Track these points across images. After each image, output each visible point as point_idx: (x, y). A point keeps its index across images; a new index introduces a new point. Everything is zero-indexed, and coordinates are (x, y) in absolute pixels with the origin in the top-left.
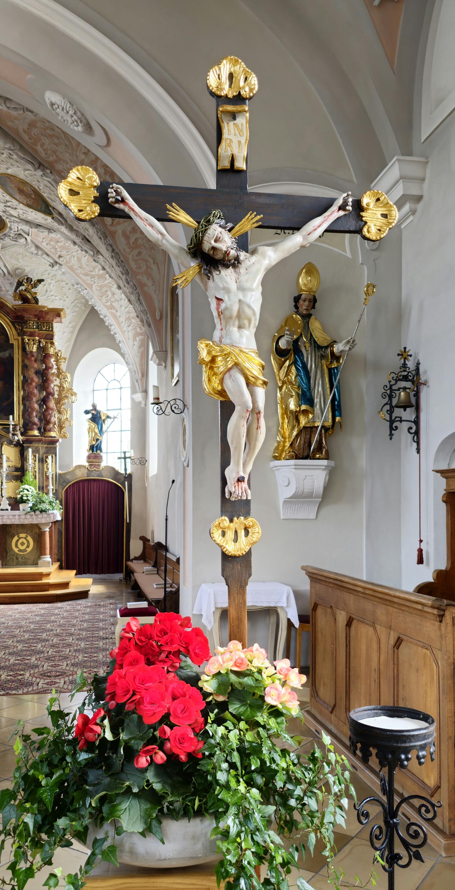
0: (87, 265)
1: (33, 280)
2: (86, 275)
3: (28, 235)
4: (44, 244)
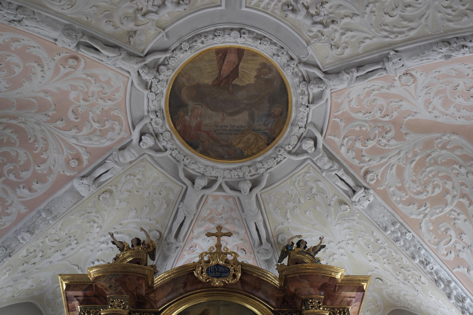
0: (414, 181)
1: (309, 246)
2: (410, 202)
3: (322, 133)
4: (343, 150)
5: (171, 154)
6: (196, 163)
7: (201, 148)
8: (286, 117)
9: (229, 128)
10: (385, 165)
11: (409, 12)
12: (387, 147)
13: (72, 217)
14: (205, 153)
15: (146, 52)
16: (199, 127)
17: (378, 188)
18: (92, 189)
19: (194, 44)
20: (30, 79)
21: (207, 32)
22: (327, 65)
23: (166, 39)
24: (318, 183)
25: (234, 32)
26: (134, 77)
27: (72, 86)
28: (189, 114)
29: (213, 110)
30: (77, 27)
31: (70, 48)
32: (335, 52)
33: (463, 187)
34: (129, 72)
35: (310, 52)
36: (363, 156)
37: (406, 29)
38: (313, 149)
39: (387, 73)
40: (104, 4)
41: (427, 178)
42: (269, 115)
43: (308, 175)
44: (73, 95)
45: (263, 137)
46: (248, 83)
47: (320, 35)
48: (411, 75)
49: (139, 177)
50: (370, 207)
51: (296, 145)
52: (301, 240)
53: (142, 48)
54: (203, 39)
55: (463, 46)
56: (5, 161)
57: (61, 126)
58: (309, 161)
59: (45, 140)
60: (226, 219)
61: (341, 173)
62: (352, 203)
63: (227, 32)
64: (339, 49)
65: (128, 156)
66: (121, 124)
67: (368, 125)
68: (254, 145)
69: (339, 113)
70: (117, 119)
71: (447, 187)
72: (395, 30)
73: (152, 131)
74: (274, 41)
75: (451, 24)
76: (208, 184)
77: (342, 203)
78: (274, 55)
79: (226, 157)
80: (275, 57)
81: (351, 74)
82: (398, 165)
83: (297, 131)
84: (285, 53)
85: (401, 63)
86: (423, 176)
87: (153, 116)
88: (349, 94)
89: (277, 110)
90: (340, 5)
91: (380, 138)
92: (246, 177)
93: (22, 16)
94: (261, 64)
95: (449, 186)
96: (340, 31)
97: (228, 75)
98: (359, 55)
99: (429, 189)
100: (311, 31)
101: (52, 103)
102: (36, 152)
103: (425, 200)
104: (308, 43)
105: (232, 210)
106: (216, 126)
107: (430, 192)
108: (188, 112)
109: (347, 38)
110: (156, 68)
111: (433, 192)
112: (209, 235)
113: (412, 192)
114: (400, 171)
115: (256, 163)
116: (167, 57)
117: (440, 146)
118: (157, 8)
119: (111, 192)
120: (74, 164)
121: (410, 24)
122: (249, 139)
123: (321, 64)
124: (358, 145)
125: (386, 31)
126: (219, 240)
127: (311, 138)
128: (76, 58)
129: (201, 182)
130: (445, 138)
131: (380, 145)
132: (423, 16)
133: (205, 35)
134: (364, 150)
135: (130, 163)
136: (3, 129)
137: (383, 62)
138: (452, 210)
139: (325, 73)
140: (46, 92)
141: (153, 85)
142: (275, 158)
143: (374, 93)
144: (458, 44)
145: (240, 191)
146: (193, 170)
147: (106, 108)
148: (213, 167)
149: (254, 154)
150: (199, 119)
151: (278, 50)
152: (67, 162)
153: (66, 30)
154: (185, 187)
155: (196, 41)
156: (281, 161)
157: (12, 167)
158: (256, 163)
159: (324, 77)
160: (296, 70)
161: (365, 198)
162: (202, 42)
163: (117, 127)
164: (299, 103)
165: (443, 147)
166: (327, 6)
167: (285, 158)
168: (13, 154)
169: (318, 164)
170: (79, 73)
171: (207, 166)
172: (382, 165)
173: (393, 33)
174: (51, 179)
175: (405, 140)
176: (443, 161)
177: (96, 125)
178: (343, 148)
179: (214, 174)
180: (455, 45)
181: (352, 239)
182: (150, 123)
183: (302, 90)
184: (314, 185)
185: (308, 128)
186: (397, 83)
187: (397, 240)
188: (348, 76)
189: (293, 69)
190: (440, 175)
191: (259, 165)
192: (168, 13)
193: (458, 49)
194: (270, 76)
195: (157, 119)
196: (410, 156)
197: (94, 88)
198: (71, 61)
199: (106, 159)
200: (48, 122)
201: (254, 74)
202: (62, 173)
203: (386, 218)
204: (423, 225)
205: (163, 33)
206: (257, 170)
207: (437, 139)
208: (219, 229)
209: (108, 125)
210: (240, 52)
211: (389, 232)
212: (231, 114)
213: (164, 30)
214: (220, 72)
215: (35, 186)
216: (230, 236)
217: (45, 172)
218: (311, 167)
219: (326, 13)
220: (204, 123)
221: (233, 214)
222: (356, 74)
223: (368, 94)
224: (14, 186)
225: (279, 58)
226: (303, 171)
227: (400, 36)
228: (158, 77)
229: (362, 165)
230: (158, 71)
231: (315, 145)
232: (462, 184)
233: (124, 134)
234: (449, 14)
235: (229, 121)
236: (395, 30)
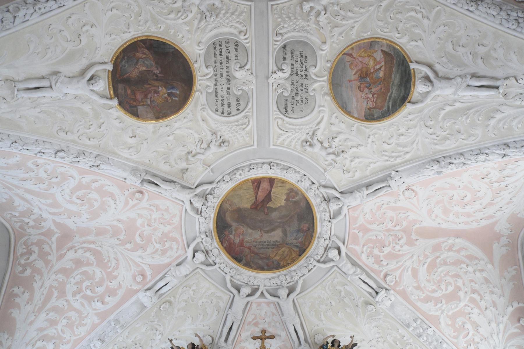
0: (428, 281)
1: (342, 344)
2: (427, 300)
3: (344, 243)
5: (220, 268)
6: (240, 274)
7: (244, 261)
8: (313, 231)
9: (266, 244)
10: (401, 268)
11: (402, 140)
12: (401, 252)
13: (137, 326)
14: (248, 265)
15: (195, 185)
16: (241, 243)
17: (398, 289)
18: (154, 301)
19: (234, 176)
20: (106, 211)
21: (243, 167)
22: (343, 186)
23: (211, 174)
24: (346, 286)
25: (265, 165)
26: (187, 205)
27: (138, 214)
28: (233, 233)
29: (252, 229)
30: (141, 168)
31: (136, 184)
32: (348, 175)
33: (472, 284)
34: (183, 202)
35: (328, 177)
36: (381, 261)
37: (402, 153)
38: (338, 257)
39: (392, 189)
40: (163, 150)
41: (439, 278)
42: (299, 231)
43: (336, 280)
44: (139, 222)
45: (295, 249)
46: (279, 205)
47: (333, 163)
48: (412, 190)
49: (194, 288)
50: (392, 306)
51: (323, 255)
52: (335, 340)
53: (193, 181)
54: (241, 172)
55: (450, 163)
56: (84, 279)
57: (129, 248)
58: (335, 268)
59: (117, 260)
60: (269, 323)
61: (364, 277)
62: (376, 304)
63: (260, 165)
64: (351, 173)
65: (184, 270)
66: (177, 243)
67: (382, 234)
68: (288, 257)
69: (357, 225)
70: (174, 239)
71: (458, 284)
72: (394, 154)
73: (203, 249)
74: (298, 170)
75: (437, 147)
76: (251, 293)
77: (368, 303)
78: (299, 181)
79: (266, 268)
80: (299, 183)
81: (362, 192)
82: (412, 268)
83: (323, 243)
84: (307, 179)
85: (402, 180)
86: (436, 276)
87: (203, 236)
88: (363, 208)
89: (305, 226)
90: (347, 139)
91: (394, 245)
92: (283, 285)
93: (100, 162)
94: (288, 190)
95: (460, 283)
96: (350, 159)
97: (263, 200)
98: (367, 177)
99: (443, 286)
100: (327, 161)
101: (123, 229)
102: (109, 270)
103: (440, 297)
104: (325, 170)
105: (273, 314)
106: (256, 242)
107: (444, 290)
108: (232, 232)
109: (355, 163)
110: (205, 197)
111: (447, 290)
112: (255, 338)
113: (428, 291)
114: (415, 273)
115: (290, 271)
116: (213, 188)
117: (447, 248)
118: (203, 150)
119: (170, 303)
120: (139, 279)
121: (404, 149)
122: (284, 252)
123: (337, 185)
124: (376, 251)
125: (386, 156)
126: (263, 343)
127: (335, 248)
128: (141, 192)
129: (246, 291)
130: (451, 241)
131: (395, 250)
132: (414, 142)
133: (242, 168)
134: (381, 256)
135: (186, 276)
136: (84, 253)
137: (387, 180)
138: (466, 305)
139: (341, 193)
140: (118, 220)
141: (203, 211)
142: (306, 267)
143: (384, 207)
144: (446, 162)
145: (279, 297)
146: (239, 280)
147: (165, 232)
148: (255, 277)
149: (288, 264)
150: (241, 237)
151: (301, 177)
152: (134, 278)
153: (133, 170)
154: (232, 296)
155: (235, 174)
156: (311, 269)
157: (89, 284)
158: (290, 271)
159: (341, 197)
160: (317, 192)
161: (387, 298)
162: (240, 175)
163: (175, 247)
164: (323, 219)
165: (450, 249)
166: (336, 140)
167: (315, 266)
168: (90, 273)
169: (343, 270)
170: (144, 204)
171: (250, 276)
172: (399, 268)
173: (392, 157)
174: (121, 293)
175: (416, 245)
176: (452, 261)
177: (158, 246)
178: (363, 255)
179: (256, 283)
180: (443, 163)
181: (381, 337)
182: (202, 242)
183: (324, 208)
184: (341, 289)
185: (332, 240)
186: (401, 197)
187: (420, 336)
188: (359, 194)
189: (315, 191)
190: (450, 274)
191: (293, 274)
192: (213, 154)
193: (446, 166)
194: (297, 198)
195: (207, 238)
196: (422, 259)
197: (156, 215)
198: (138, 195)
199: (166, 274)
200: (120, 244)
201: (284, 197)
202: (129, 287)
203: (408, 316)
204: (442, 320)
205: (209, 169)
206: (292, 278)
207: (443, 243)
208: (263, 333)
209: (167, 245)
210: (271, 181)
211: (412, 329)
212: (267, 232)
213: (209, 167)
214: (256, 198)
215: (107, 299)
216: (272, 339)
217: (116, 287)
218: (338, 274)
219: (337, 145)
220: (245, 240)
221: (274, 318)
222: (366, 192)
223: (379, 208)
224: (89, 299)
225: (303, 183)
226: (332, 276)
227: (398, 159)
228: (207, 204)
229: (381, 269)
230: (206, 199)
231: (340, 254)
232: (472, 281)
233: (180, 252)
234: (434, 139)
235: (267, 238)
236: (394, 154)
